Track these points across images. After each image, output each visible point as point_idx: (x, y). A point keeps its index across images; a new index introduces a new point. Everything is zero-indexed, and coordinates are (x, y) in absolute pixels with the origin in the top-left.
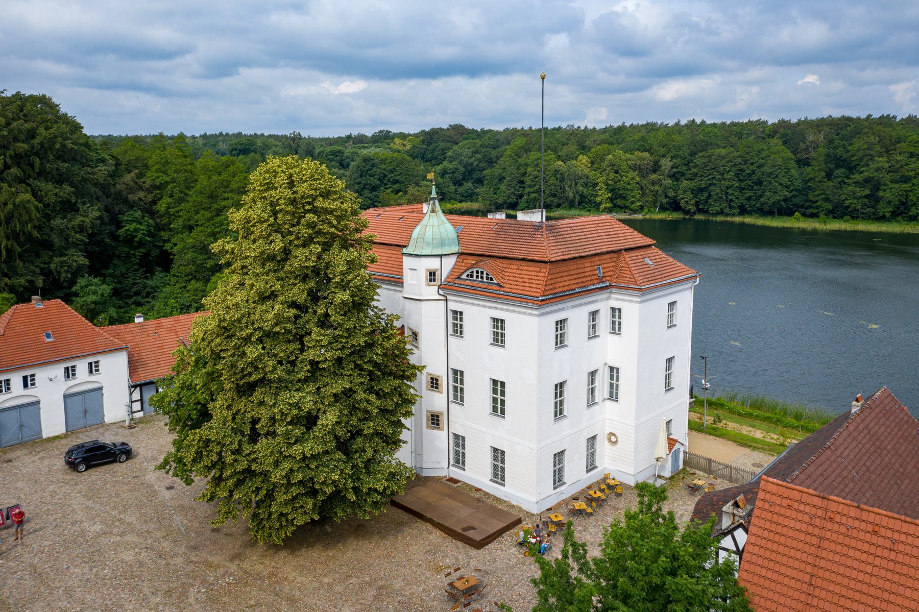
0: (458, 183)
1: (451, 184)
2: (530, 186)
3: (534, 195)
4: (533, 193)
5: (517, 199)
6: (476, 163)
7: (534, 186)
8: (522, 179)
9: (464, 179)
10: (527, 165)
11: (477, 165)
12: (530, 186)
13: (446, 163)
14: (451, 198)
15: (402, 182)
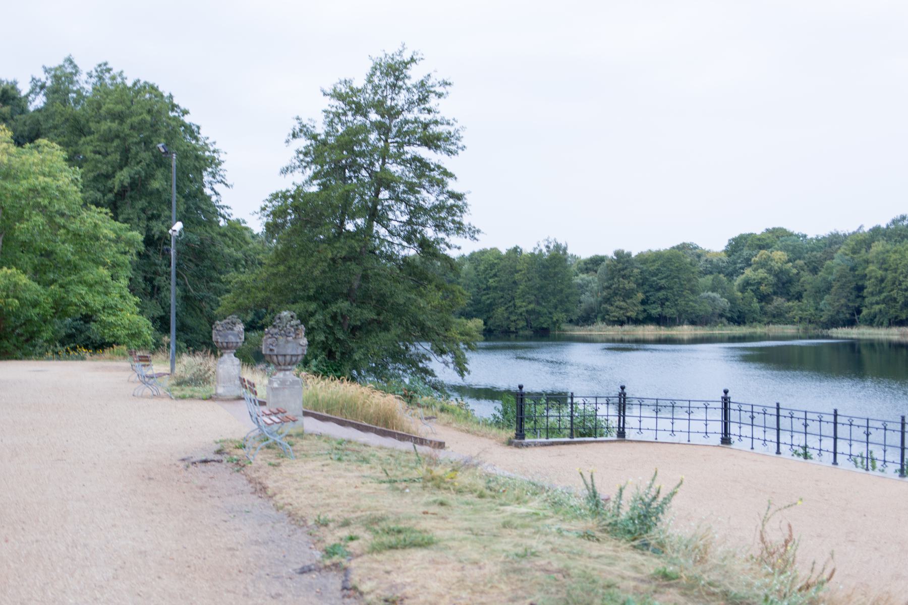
0: (764, 298)
1: (755, 299)
2: (872, 294)
3: (877, 308)
4: (877, 303)
5: (853, 315)
6: (795, 271)
7: (880, 292)
8: (860, 283)
9: (775, 293)
10: (867, 262)
11: (798, 274)
12: (872, 294)
13: (748, 272)
14: (754, 320)
15: (672, 288)
